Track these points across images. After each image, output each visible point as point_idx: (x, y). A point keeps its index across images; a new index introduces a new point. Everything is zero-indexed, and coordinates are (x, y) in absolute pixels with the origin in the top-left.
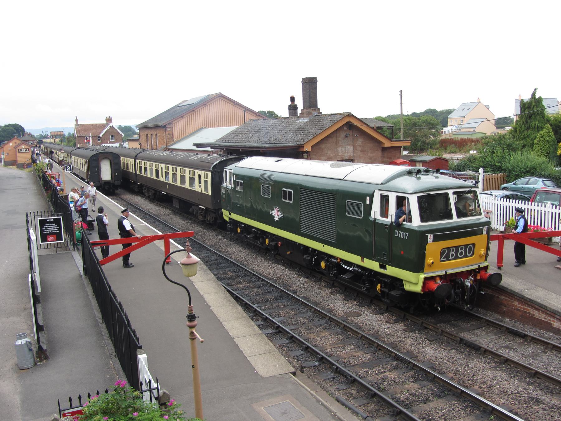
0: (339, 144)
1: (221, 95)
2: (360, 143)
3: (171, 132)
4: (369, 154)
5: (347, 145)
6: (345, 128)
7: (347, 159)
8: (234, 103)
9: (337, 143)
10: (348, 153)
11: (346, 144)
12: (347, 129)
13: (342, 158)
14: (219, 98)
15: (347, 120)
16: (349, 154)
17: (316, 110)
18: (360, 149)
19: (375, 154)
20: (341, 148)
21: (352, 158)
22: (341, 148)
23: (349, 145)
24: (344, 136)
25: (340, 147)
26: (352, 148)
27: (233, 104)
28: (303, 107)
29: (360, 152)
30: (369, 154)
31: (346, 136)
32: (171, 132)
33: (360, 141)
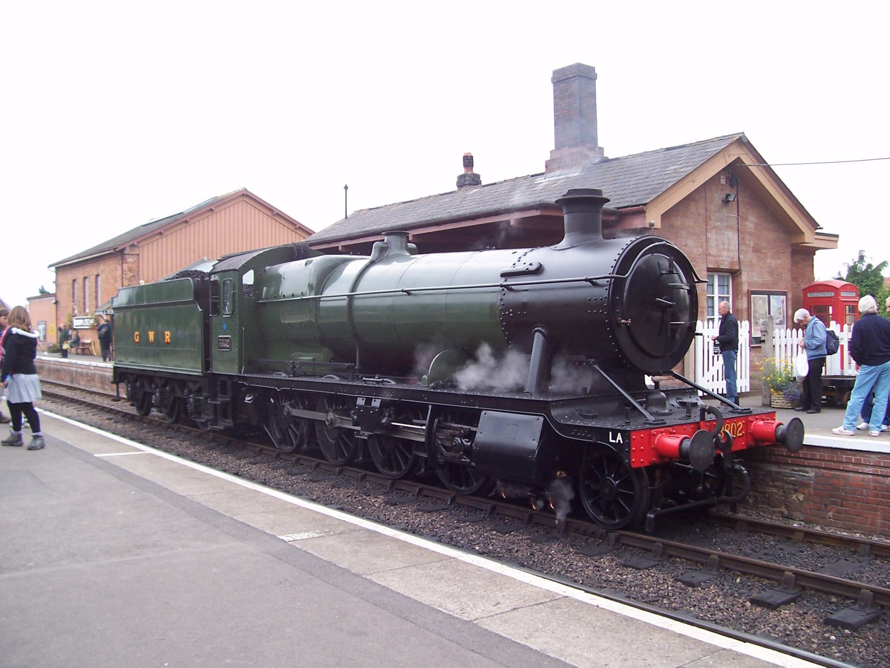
0: (710, 222)
1: (245, 193)
2: (752, 226)
3: (134, 266)
4: (769, 260)
5: (727, 227)
6: (723, 181)
7: (728, 267)
8: (272, 211)
9: (707, 220)
10: (728, 250)
11: (725, 224)
12: (726, 183)
13: (717, 262)
14: (241, 199)
15: (736, 153)
16: (731, 254)
17: (597, 149)
18: (752, 244)
19: (780, 261)
20: (716, 233)
21: (737, 267)
22: (716, 233)
23: (732, 228)
24: (720, 202)
25: (714, 231)
26: (736, 237)
27: (270, 214)
28: (556, 145)
29: (751, 250)
30: (769, 260)
31: (726, 202)
32: (134, 266)
33: (751, 222)
